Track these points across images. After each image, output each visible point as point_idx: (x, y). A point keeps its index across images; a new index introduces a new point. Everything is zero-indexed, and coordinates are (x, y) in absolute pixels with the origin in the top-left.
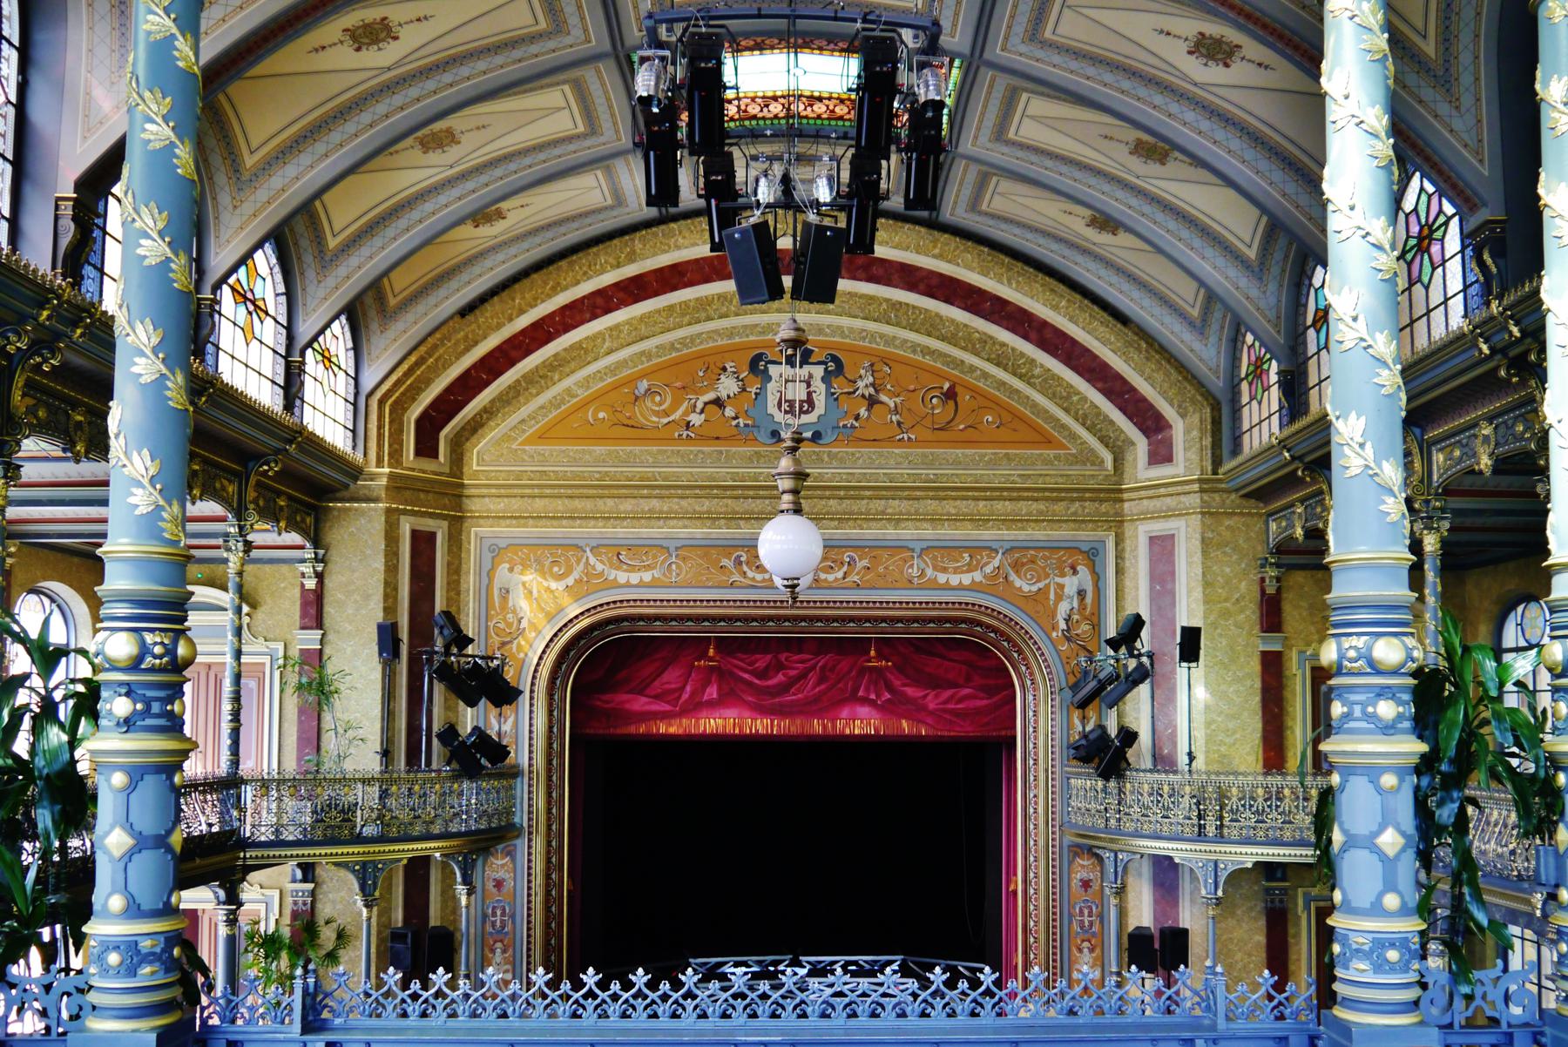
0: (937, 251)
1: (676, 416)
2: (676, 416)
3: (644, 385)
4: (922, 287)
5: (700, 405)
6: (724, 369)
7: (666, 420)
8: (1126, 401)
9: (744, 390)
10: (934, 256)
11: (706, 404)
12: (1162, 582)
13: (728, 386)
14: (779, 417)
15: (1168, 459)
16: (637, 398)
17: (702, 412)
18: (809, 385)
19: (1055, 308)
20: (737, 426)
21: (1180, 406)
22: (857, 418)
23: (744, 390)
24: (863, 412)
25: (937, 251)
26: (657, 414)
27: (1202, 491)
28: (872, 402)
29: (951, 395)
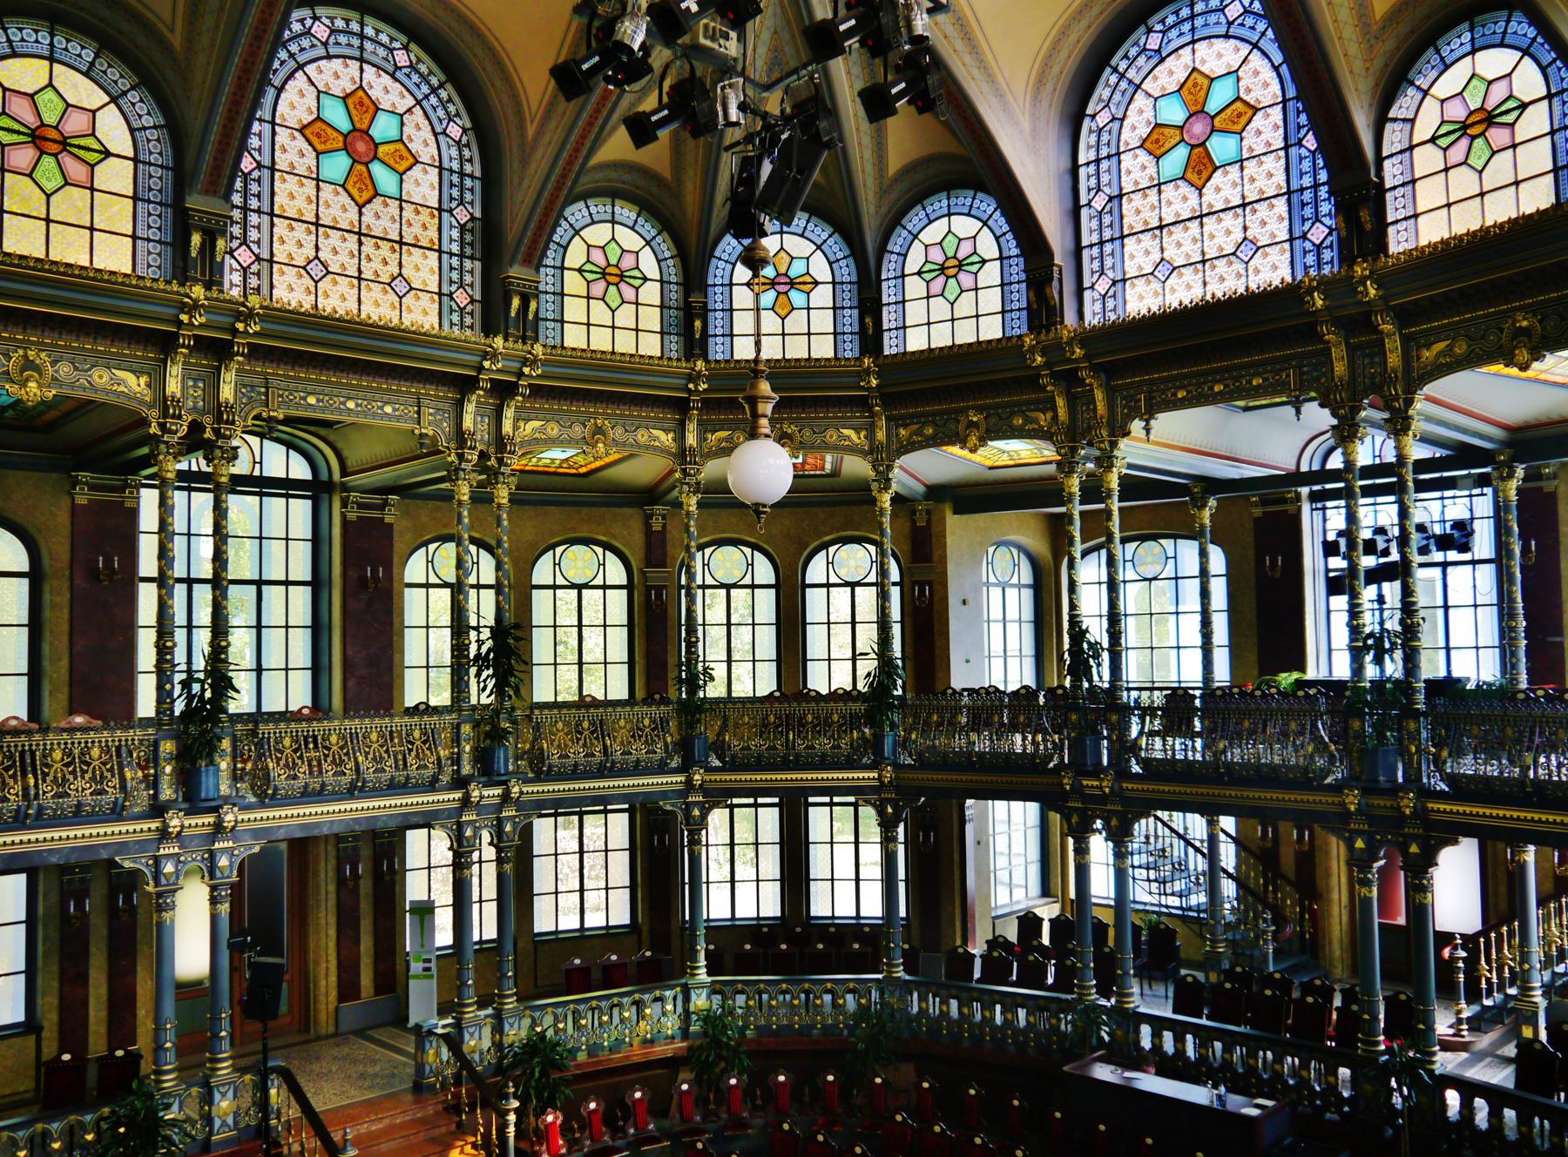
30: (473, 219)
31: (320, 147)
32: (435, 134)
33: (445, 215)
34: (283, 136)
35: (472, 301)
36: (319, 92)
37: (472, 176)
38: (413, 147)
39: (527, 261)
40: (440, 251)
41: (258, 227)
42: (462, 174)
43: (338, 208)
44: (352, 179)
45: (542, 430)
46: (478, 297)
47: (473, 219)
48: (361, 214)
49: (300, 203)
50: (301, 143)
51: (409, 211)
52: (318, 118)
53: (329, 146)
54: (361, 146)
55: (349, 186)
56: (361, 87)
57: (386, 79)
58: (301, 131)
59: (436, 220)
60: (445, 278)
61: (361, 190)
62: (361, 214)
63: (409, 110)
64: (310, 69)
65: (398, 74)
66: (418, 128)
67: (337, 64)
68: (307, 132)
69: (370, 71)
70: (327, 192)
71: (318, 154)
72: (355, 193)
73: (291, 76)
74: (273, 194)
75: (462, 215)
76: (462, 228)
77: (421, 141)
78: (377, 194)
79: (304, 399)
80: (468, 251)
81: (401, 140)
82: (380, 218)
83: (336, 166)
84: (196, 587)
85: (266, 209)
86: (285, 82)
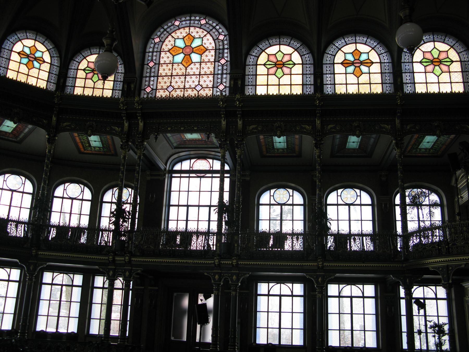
31: (174, 54)
32: (214, 40)
34: (163, 54)
35: (225, 87)
36: (175, 39)
38: (205, 46)
40: (214, 74)
41: (153, 81)
43: (179, 69)
45: (256, 128)
46: (228, 85)
48: (186, 69)
49: (167, 71)
50: (168, 54)
52: (175, 46)
53: (177, 53)
55: (183, 63)
56: (189, 34)
57: (198, 29)
58: (169, 51)
59: (213, 65)
61: (187, 63)
62: (186, 69)
63: (205, 36)
64: (173, 34)
65: (202, 27)
67: (182, 30)
68: (171, 51)
69: (192, 29)
70: (175, 66)
71: (173, 56)
72: (185, 64)
73: (167, 37)
74: (159, 70)
79: (167, 128)
81: (202, 45)
82: (193, 69)
84: (190, 208)
86: (165, 39)
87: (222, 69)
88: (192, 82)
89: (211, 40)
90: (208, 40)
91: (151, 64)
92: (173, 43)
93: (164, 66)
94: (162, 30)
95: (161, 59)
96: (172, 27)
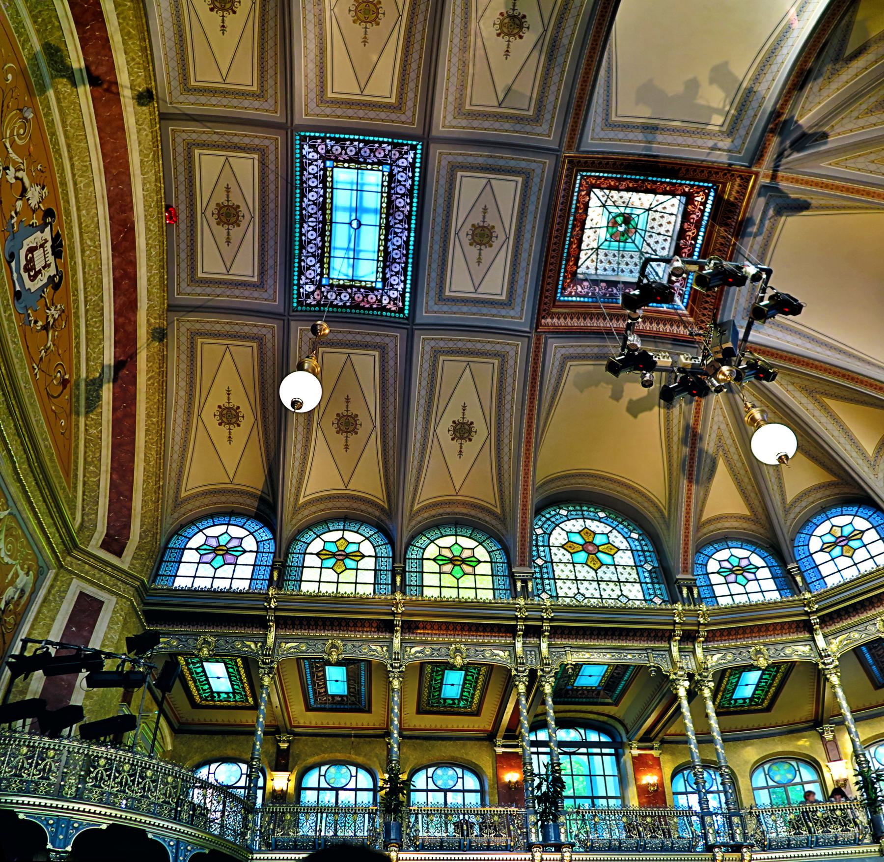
0: (152, 321)
1: (13, 156)
2: (13, 156)
3: (31, 116)
4: (121, 320)
5: (20, 174)
6: (43, 188)
7: (8, 145)
8: (118, 499)
9: (34, 211)
10: (148, 320)
11: (21, 180)
12: (80, 627)
13: (34, 195)
14: (23, 253)
15: (119, 553)
16: (21, 110)
17: (17, 178)
18: (44, 268)
19: (148, 416)
20: (12, 217)
21: (144, 532)
22: (36, 322)
23: (34, 211)
24: (40, 323)
25: (152, 321)
26: (12, 135)
27: (137, 589)
28: (46, 328)
29: (64, 383)
30: (654, 567)
33: (639, 569)
34: (554, 550)
37: (648, 551)
39: (685, 571)
42: (643, 551)
44: (590, 560)
47: (654, 567)
51: (620, 569)
52: (569, 541)
54: (591, 548)
57: (596, 523)
58: (562, 547)
60: (646, 592)
63: (611, 532)
64: (562, 525)
66: (616, 537)
67: (573, 522)
69: (588, 522)
70: (578, 567)
72: (592, 565)
73: (554, 529)
74: (554, 571)
75: (648, 567)
76: (650, 572)
77: (618, 540)
78: (603, 565)
80: (655, 580)
82: (607, 573)
83: (582, 557)
85: (551, 576)
87: (651, 578)
88: (610, 592)
89: (620, 538)
90: (616, 537)
91: (540, 562)
92: (566, 537)
93: (561, 566)
94: (543, 519)
95: (553, 557)
96: (558, 517)
